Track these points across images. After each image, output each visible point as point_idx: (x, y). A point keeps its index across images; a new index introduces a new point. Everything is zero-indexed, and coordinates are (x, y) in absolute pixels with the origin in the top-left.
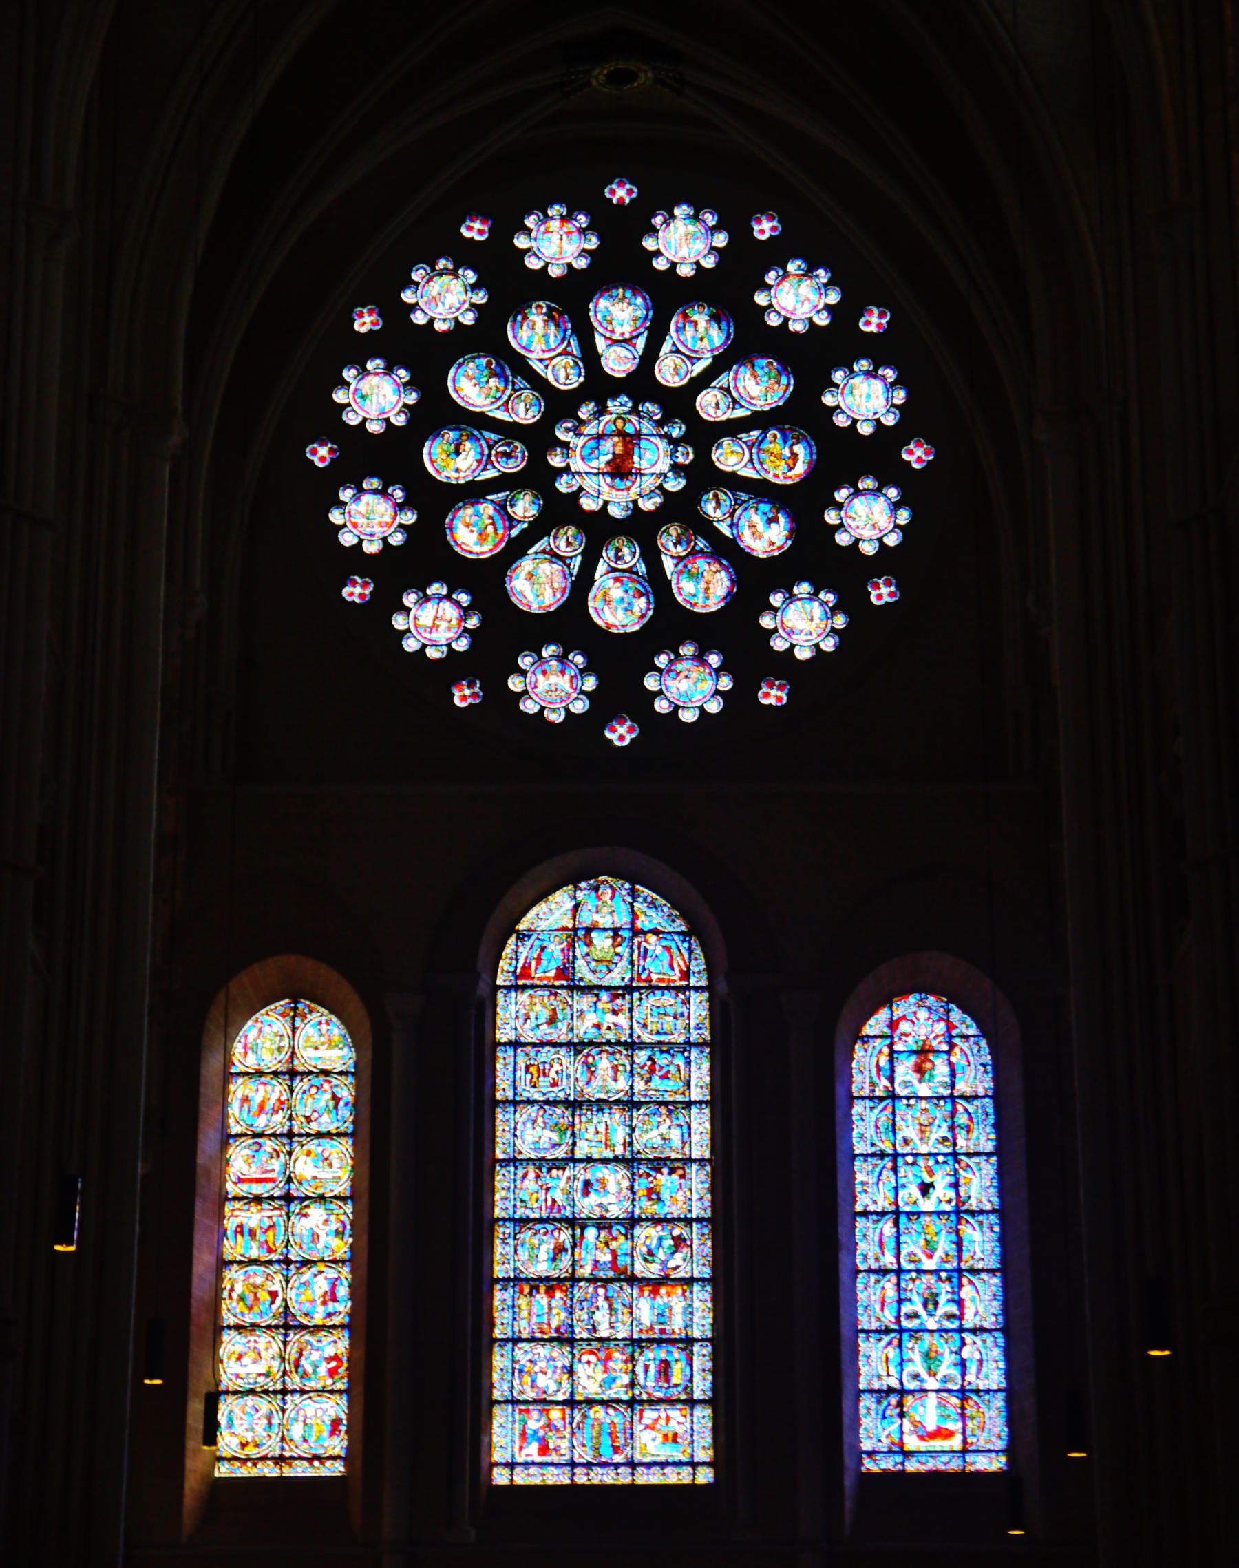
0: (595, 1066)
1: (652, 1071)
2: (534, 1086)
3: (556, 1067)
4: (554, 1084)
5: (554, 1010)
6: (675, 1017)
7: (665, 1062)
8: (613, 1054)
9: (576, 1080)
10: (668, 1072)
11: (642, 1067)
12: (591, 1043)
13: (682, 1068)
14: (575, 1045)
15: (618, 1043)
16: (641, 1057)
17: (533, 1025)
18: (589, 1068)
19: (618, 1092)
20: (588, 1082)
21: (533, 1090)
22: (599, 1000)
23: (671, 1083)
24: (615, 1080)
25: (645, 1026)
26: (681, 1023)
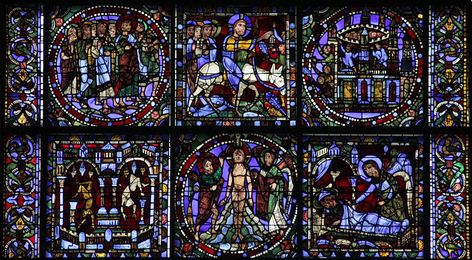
0: (220, 183)
1: (343, 194)
2: (86, 229)
3: (135, 182)
4: (128, 222)
5: (131, 55)
6: (393, 70)
7: (372, 171)
8: (257, 154)
9: (177, 213)
10: (378, 193)
11: (321, 184)
12: (210, 129)
13: (409, 185)
14: (176, 131)
15: (269, 127)
16: (322, 160)
17: (83, 87)
18: (205, 186)
19: (270, 238)
20: (203, 219)
21: (82, 237)
22: (228, 31)
23: (383, 221)
24: (264, 215)
25: (326, 90)
26: (402, 85)
